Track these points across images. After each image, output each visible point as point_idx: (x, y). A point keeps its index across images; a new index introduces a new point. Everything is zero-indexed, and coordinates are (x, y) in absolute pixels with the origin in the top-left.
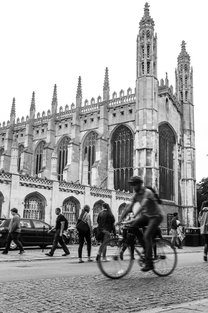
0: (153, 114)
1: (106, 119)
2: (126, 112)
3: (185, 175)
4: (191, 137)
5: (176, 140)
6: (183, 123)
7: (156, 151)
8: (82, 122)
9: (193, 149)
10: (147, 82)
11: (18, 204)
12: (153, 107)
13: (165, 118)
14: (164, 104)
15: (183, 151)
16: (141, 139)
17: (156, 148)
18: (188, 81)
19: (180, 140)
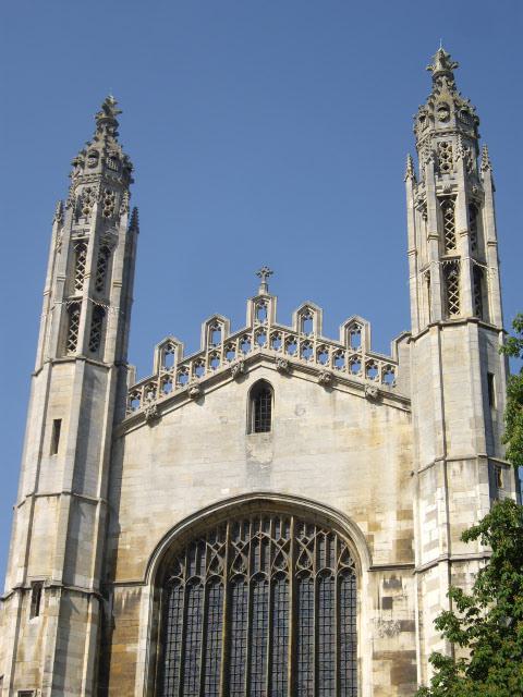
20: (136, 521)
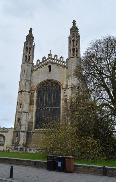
5: (61, 87)
20: (34, 83)
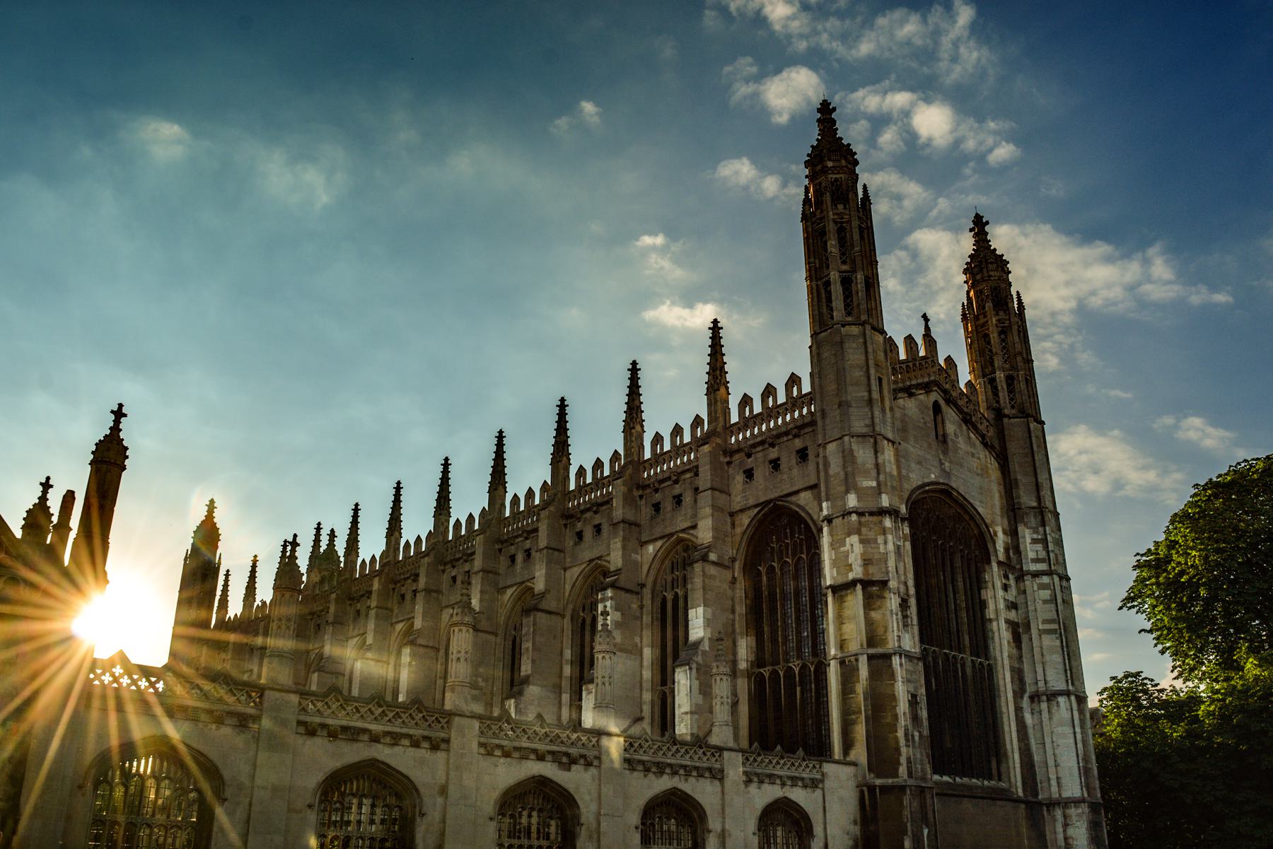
0: (879, 454)
1: (720, 489)
2: (788, 460)
3: (1040, 677)
4: (1048, 532)
5: (991, 550)
6: (1009, 486)
7: (902, 589)
8: (646, 511)
9: (1061, 578)
10: (847, 345)
11: (288, 812)
12: (877, 428)
13: (933, 470)
14: (927, 419)
15: (1022, 589)
16: (842, 549)
17: (903, 578)
18: (1010, 339)
19: (1007, 550)
